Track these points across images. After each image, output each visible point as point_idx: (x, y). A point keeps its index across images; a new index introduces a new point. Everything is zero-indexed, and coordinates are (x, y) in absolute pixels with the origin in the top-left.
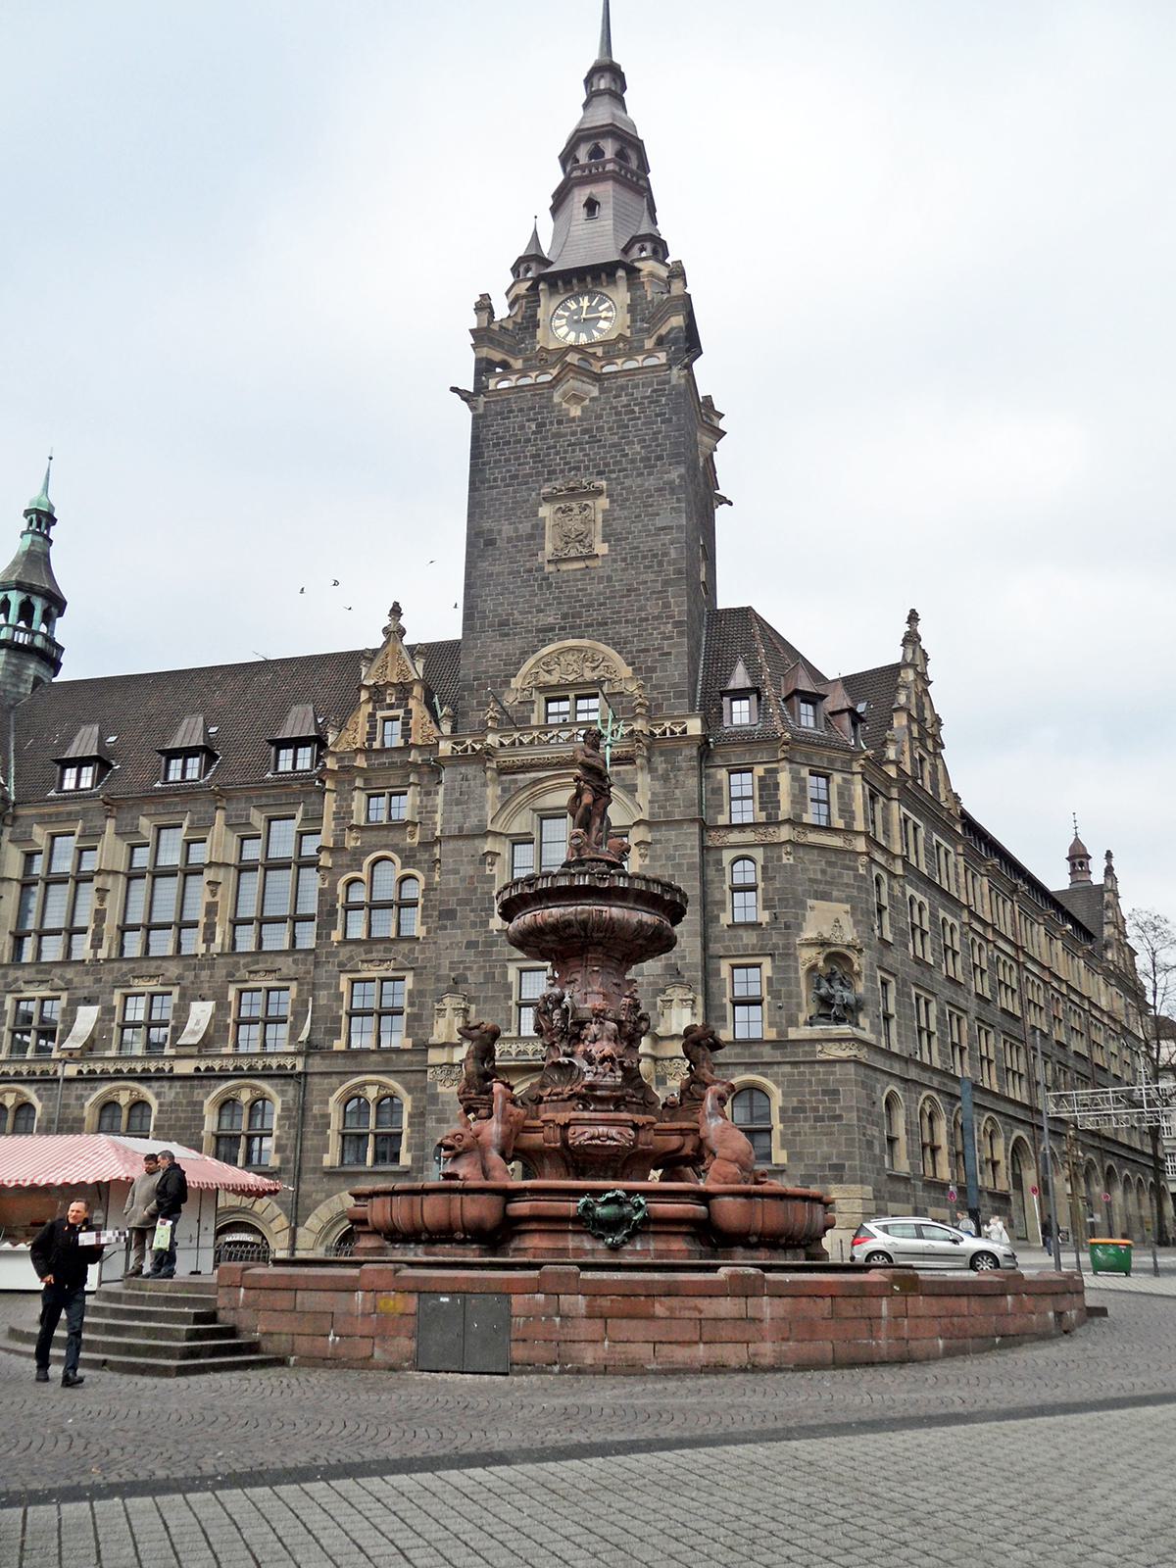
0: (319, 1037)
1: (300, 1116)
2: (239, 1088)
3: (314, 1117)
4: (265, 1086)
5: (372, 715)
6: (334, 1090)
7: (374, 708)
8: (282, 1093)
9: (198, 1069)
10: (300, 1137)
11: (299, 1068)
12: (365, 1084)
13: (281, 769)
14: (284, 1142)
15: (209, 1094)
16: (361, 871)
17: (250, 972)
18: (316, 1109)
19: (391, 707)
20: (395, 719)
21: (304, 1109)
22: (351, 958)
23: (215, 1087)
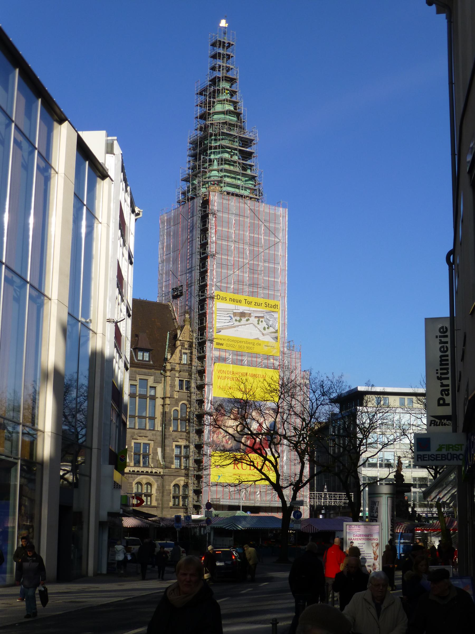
0: (168, 464)
1: (162, 489)
2: (142, 478)
3: (167, 490)
4: (151, 479)
5: (181, 351)
6: (172, 482)
7: (181, 348)
8: (157, 481)
9: (130, 471)
10: (163, 496)
11: (162, 473)
12: (179, 480)
13: (139, 359)
14: (158, 498)
15: (134, 480)
16: (178, 407)
17: (139, 436)
18: (167, 487)
19: (186, 349)
20: (186, 354)
21: (163, 486)
22: (176, 437)
23: (136, 478)
